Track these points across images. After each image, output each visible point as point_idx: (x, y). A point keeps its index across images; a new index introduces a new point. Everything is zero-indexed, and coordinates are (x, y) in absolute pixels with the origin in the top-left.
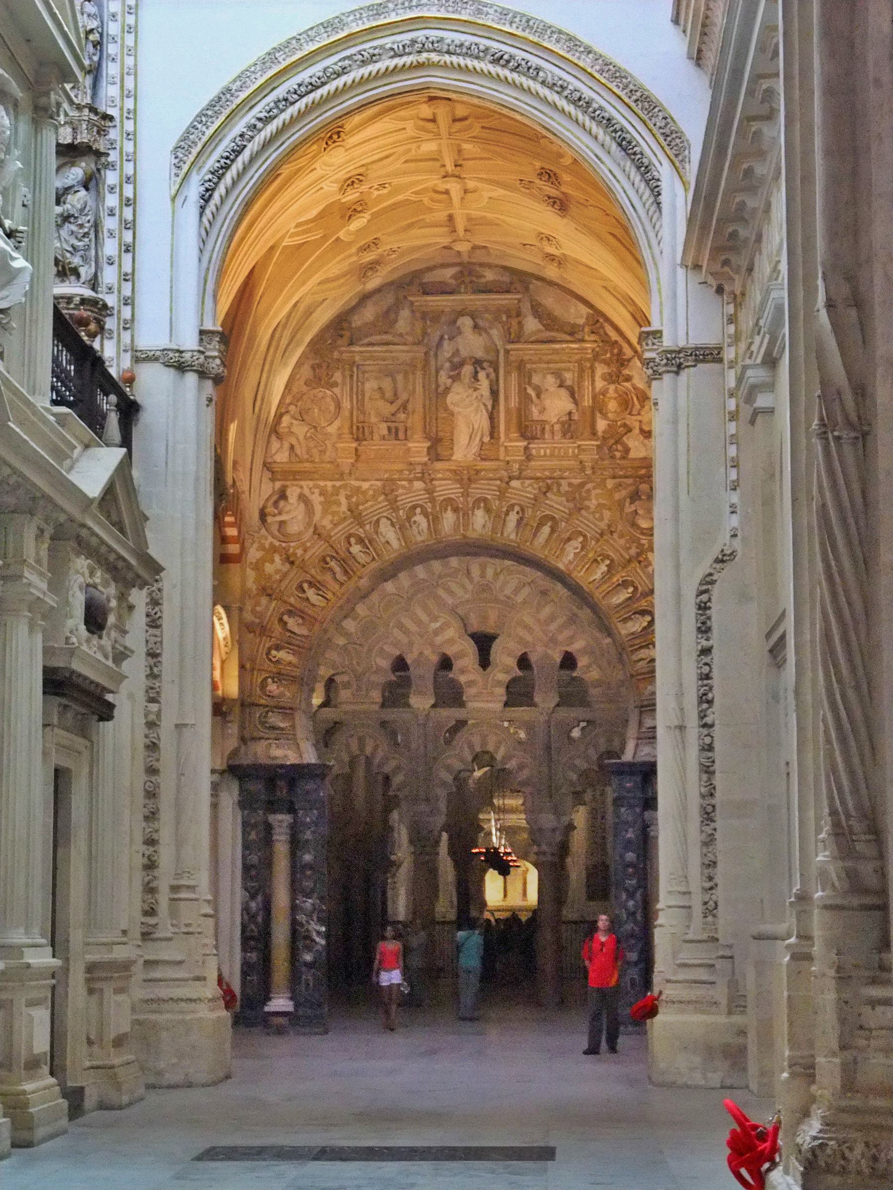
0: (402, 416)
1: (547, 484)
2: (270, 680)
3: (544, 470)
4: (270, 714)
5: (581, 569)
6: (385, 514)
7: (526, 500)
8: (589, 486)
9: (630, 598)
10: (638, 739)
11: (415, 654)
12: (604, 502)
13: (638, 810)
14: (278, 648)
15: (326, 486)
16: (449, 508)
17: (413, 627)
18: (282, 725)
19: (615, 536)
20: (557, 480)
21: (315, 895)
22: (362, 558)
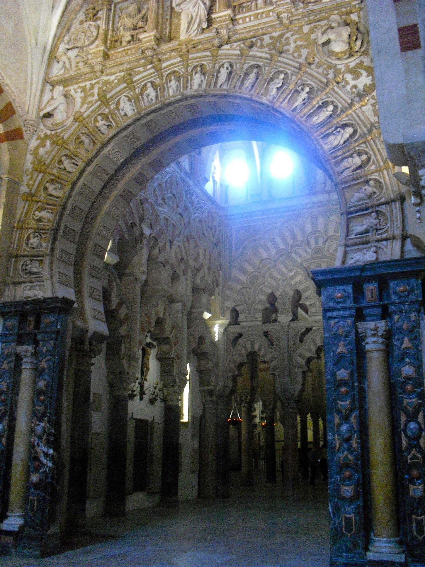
0: (141, 24)
1: (252, 42)
2: (32, 236)
3: (250, 31)
4: (29, 262)
5: (284, 100)
6: (125, 94)
7: (234, 57)
8: (288, 35)
9: (331, 116)
10: (346, 246)
11: (281, 291)
12: (302, 43)
13: (349, 321)
14: (41, 209)
15: (86, 86)
16: (173, 78)
17: (279, 277)
18: (35, 270)
19: (313, 66)
20: (260, 37)
21: (46, 419)
22: (104, 129)
